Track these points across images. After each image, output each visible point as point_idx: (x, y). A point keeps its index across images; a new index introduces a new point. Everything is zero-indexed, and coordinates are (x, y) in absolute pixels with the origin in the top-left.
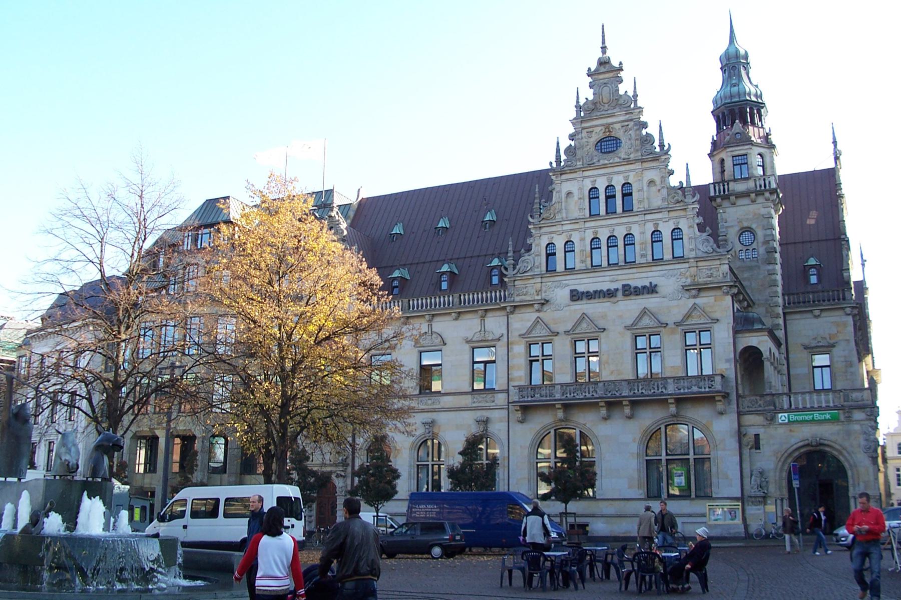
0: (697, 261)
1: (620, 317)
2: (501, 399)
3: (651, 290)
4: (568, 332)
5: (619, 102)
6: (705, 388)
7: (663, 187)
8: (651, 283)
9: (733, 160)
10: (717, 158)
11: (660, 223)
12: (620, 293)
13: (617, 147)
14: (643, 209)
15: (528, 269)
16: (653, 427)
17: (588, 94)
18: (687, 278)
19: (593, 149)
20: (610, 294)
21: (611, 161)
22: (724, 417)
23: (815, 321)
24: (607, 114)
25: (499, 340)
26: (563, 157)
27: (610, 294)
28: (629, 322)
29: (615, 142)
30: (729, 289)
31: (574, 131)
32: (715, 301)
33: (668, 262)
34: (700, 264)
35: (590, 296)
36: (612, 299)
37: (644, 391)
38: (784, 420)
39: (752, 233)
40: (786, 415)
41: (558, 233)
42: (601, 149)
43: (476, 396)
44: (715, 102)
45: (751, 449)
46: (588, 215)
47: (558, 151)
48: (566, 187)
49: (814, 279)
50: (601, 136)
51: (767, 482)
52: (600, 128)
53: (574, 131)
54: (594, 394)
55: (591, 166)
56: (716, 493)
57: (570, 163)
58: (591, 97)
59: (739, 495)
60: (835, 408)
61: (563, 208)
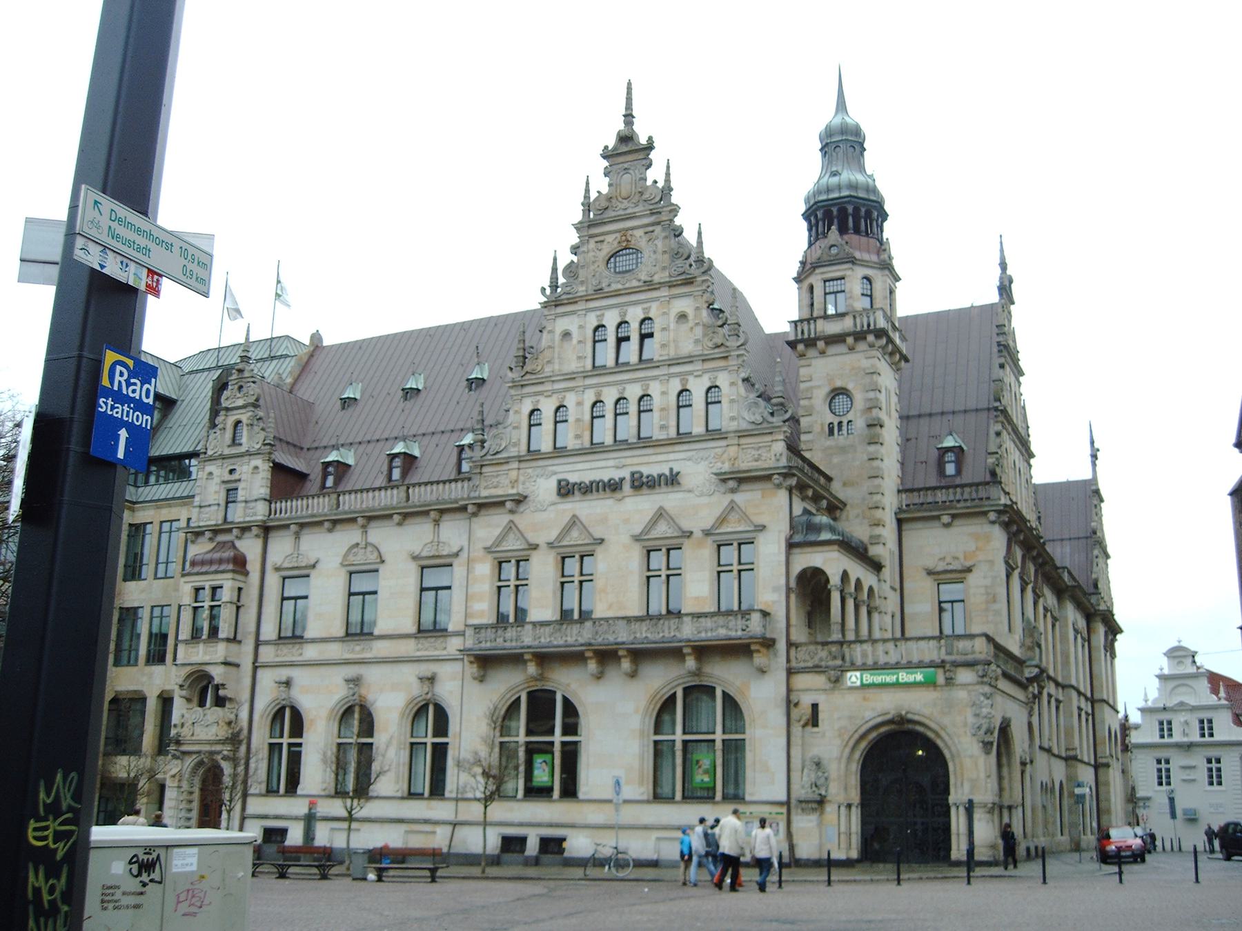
0: (739, 437)
1: (626, 521)
2: (454, 644)
3: (673, 480)
5: (644, 197)
6: (736, 631)
7: (697, 324)
8: (671, 470)
9: (825, 287)
10: (806, 284)
11: (691, 379)
12: (627, 486)
13: (637, 263)
14: (666, 358)
15: (501, 448)
16: (665, 690)
17: (601, 185)
18: (723, 463)
19: (603, 267)
20: (614, 487)
21: (627, 285)
22: (767, 677)
23: (944, 532)
24: (625, 215)
25: (457, 555)
26: (561, 280)
27: (614, 487)
28: (638, 530)
29: (635, 256)
30: (781, 479)
31: (578, 240)
33: (699, 439)
34: (743, 441)
35: (587, 489)
36: (618, 495)
37: (649, 635)
38: (855, 683)
39: (848, 396)
40: (858, 674)
41: (545, 394)
42: (615, 267)
43: (422, 641)
44: (807, 200)
45: (804, 726)
46: (589, 366)
47: (554, 270)
48: (562, 325)
49: (950, 469)
51: (826, 779)
52: (614, 236)
54: (579, 639)
55: (599, 293)
56: (752, 794)
57: (568, 289)
58: (605, 190)
59: (783, 797)
60: (932, 665)
61: (556, 356)
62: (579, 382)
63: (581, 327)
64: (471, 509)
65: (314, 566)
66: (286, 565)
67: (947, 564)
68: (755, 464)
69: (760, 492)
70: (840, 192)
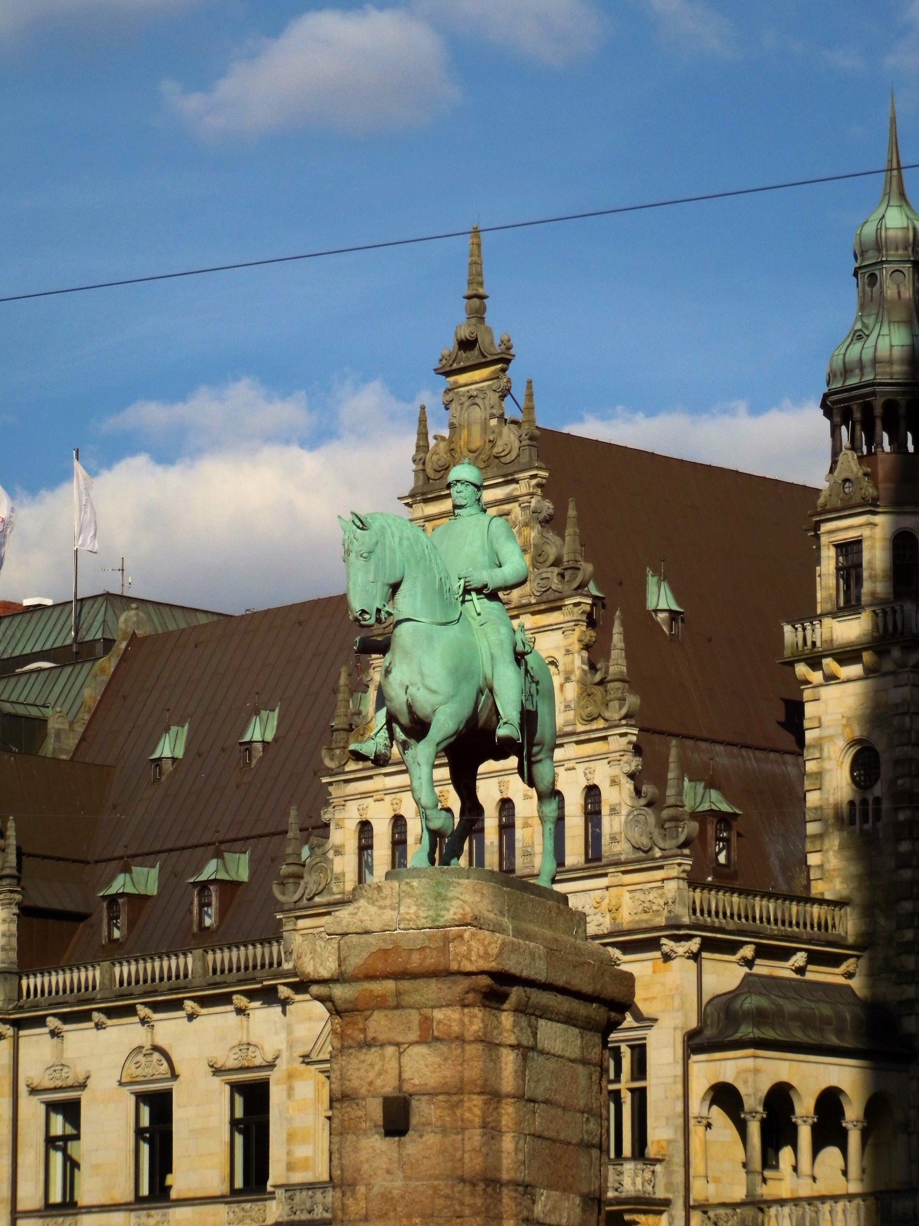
5: (495, 450)
15: (321, 888)
25: (271, 1066)
32: (654, 972)
64: (284, 992)
65: (83, 1086)
66: (48, 1084)
68: (645, 917)
69: (650, 963)
70: (862, 375)
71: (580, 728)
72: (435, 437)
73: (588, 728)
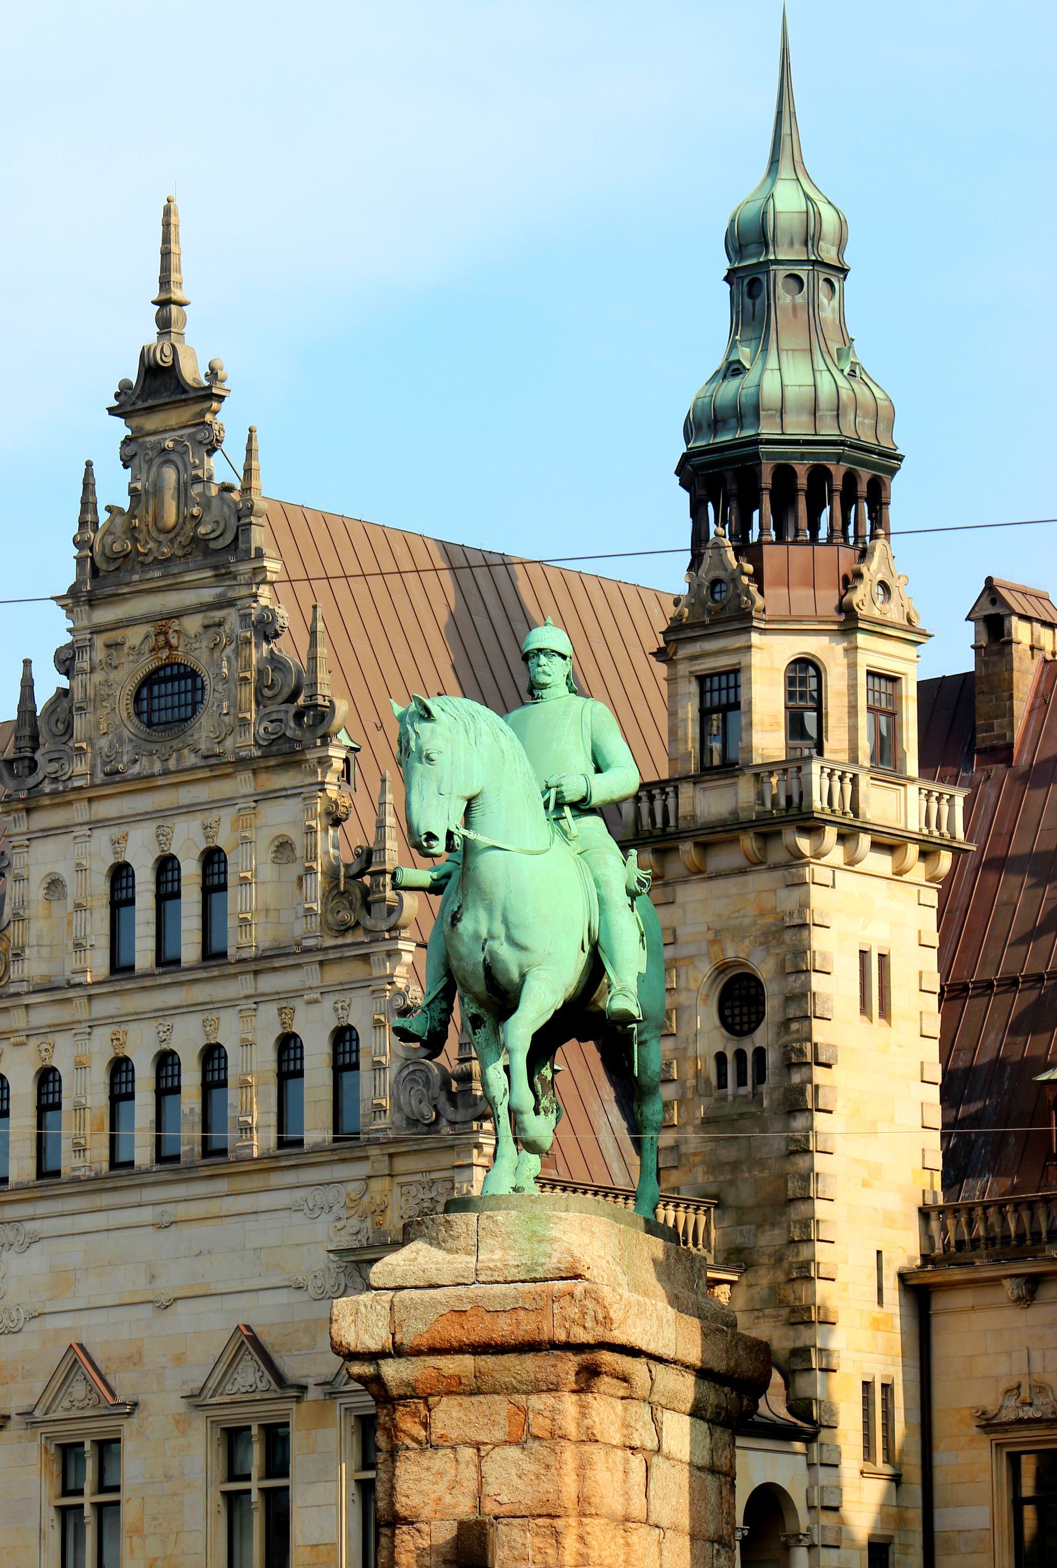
0: (391, 1156)
4: (30, 1413)
21: (172, 764)
42: (151, 711)
50: (147, 664)
52: (142, 630)
53: (68, 638)
57: (55, 766)
58: (124, 503)
62: (79, 1011)
63: (80, 868)
67: (1024, 1404)
71: (330, 942)
72: (109, 509)
73: (340, 941)
